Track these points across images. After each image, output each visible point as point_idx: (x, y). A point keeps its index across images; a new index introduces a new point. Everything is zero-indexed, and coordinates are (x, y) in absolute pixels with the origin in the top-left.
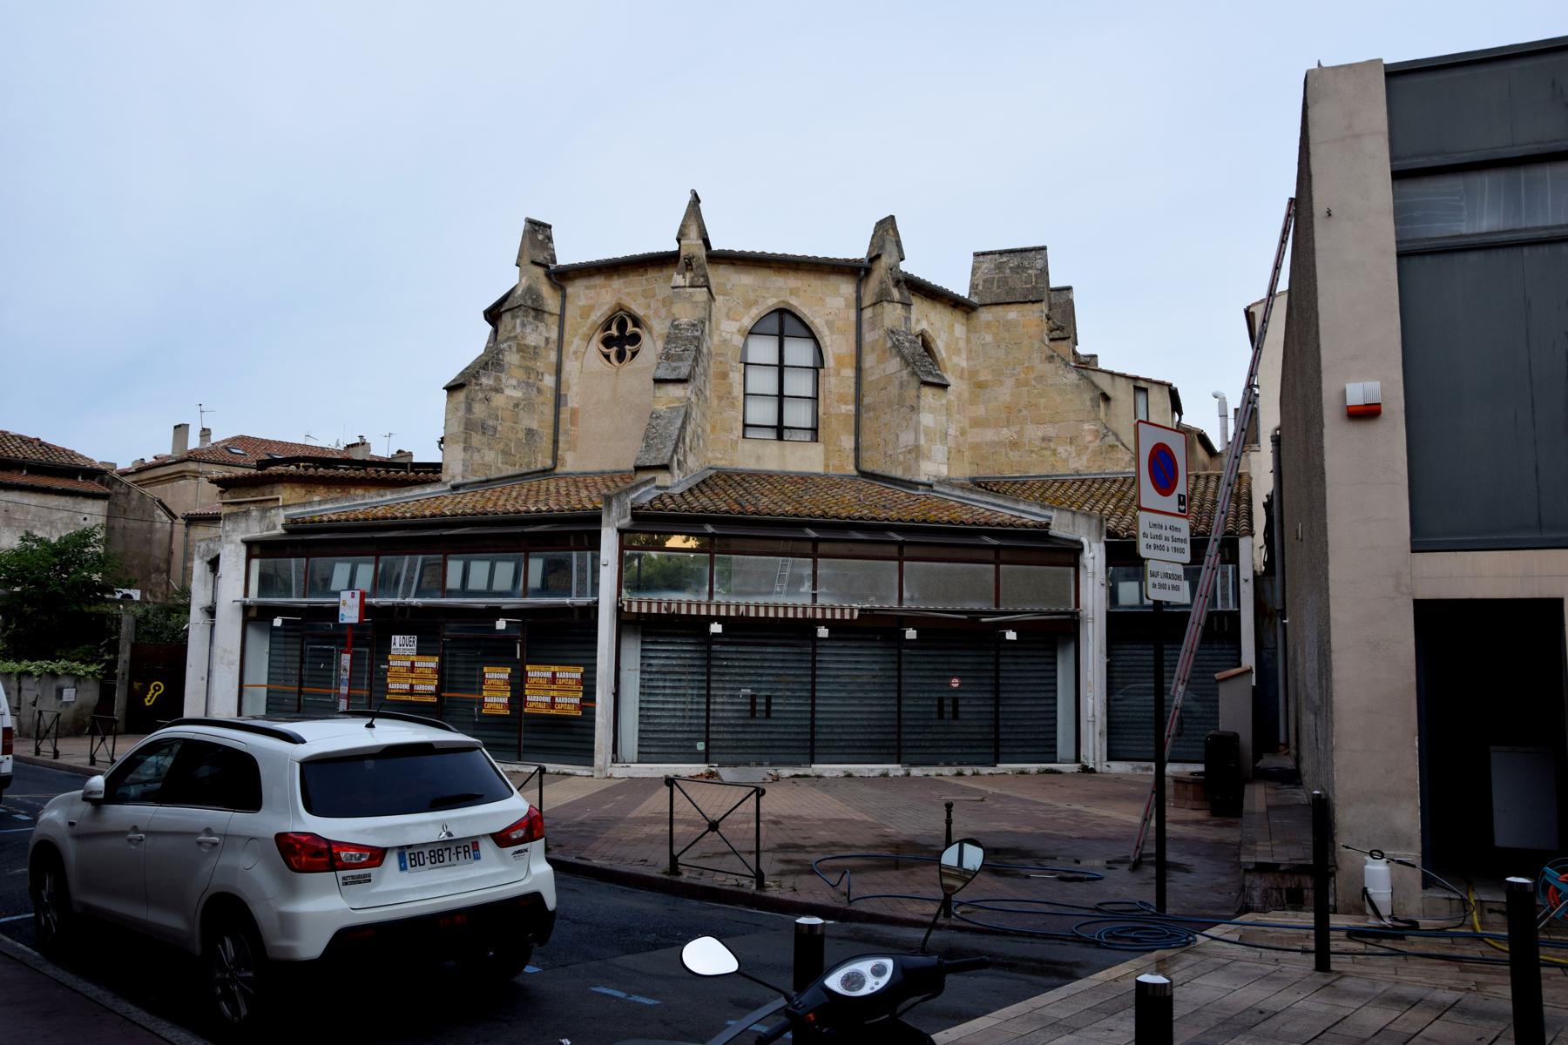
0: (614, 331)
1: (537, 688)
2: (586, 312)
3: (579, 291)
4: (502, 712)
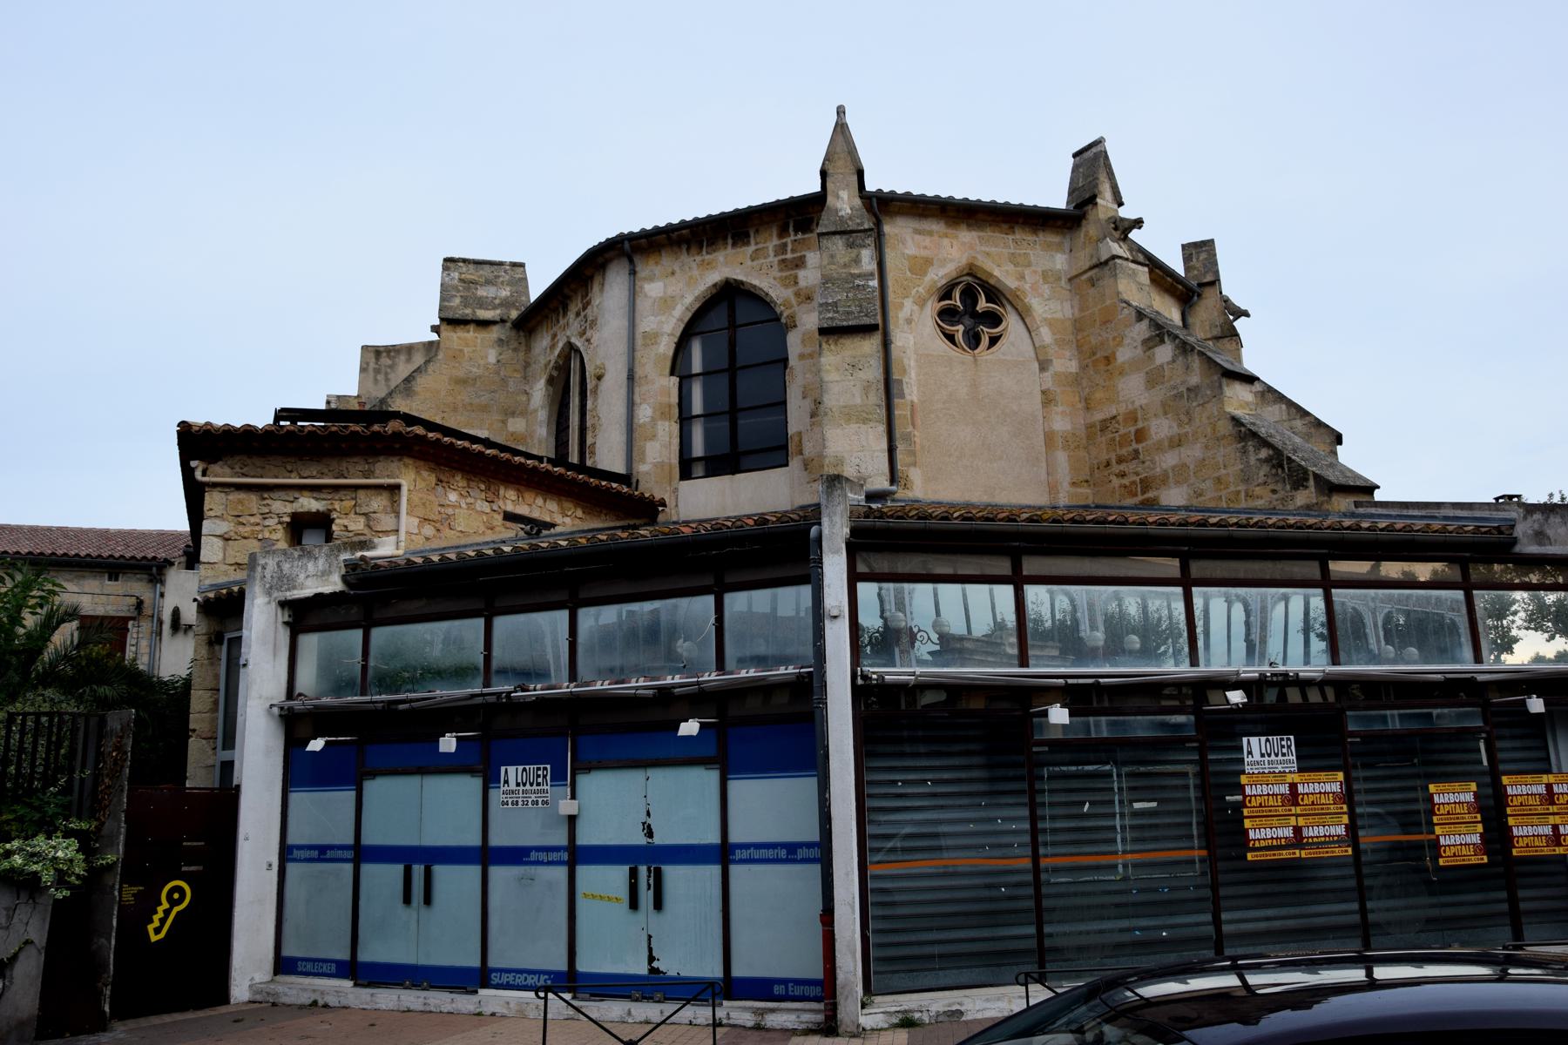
0: (956, 301)
1: (1527, 814)
2: (921, 266)
3: (903, 235)
4: (1474, 860)
